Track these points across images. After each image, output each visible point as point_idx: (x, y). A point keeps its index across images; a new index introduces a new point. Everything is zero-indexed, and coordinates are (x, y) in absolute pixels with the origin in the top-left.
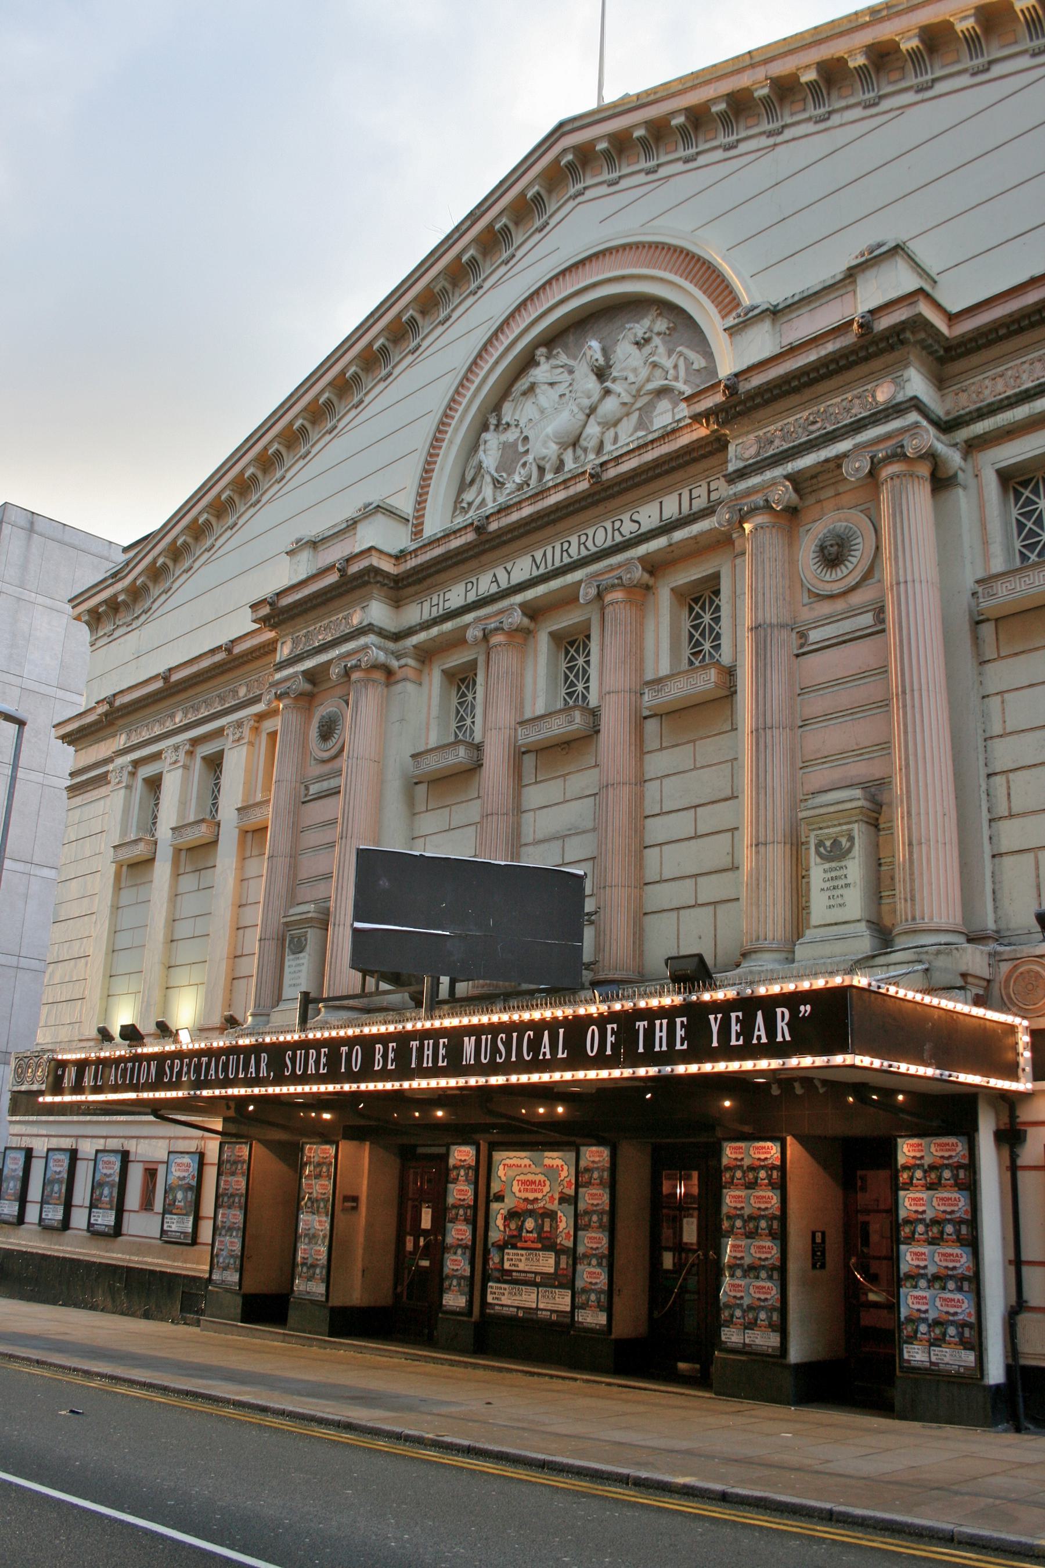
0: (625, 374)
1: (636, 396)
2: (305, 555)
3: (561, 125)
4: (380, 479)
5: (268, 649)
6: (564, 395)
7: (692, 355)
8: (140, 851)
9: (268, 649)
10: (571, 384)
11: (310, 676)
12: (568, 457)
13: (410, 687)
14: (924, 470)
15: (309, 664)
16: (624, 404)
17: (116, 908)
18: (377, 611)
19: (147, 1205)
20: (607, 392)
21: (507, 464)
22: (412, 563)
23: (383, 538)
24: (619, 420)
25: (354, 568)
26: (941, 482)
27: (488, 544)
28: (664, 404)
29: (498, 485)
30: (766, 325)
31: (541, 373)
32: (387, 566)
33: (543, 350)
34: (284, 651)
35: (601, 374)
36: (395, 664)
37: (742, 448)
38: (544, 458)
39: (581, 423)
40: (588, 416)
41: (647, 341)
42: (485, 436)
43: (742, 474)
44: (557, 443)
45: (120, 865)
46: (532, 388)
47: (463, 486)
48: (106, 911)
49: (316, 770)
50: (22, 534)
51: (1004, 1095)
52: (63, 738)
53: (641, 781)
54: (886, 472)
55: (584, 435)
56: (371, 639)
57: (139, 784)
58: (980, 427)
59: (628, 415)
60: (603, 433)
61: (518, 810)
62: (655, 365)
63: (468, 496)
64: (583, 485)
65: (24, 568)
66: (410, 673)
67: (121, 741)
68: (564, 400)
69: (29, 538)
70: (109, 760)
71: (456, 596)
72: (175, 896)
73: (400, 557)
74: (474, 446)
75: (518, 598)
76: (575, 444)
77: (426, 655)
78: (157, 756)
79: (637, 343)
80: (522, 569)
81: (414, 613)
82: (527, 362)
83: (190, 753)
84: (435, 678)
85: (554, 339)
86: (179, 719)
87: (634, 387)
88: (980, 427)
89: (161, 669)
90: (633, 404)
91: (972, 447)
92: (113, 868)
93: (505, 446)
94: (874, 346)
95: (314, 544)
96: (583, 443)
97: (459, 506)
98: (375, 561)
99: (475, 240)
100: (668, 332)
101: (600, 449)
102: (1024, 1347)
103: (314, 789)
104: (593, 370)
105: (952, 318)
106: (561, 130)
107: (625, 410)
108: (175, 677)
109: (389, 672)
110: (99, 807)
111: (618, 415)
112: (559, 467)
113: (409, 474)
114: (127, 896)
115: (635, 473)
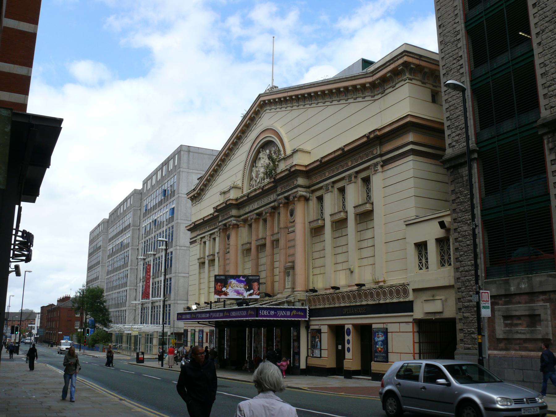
2: (223, 195)
3: (260, 95)
4: (234, 179)
5: (217, 216)
8: (202, 260)
9: (217, 216)
11: (225, 225)
13: (242, 228)
14: (302, 199)
15: (224, 222)
17: (200, 273)
18: (234, 212)
19: (207, 342)
21: (257, 177)
22: (239, 201)
23: (233, 195)
25: (228, 203)
26: (307, 199)
27: (249, 199)
29: (256, 181)
30: (283, 161)
31: (261, 155)
32: (234, 202)
33: (261, 149)
34: (220, 219)
36: (239, 223)
37: (279, 190)
42: (253, 169)
43: (278, 195)
45: (200, 263)
46: (260, 158)
47: (251, 179)
48: (198, 274)
49: (227, 246)
50: (187, 153)
51: (305, 320)
52: (188, 230)
53: (273, 254)
54: (296, 199)
56: (232, 219)
57: (202, 243)
58: (313, 188)
61: (258, 258)
63: (251, 183)
64: (261, 190)
65: (188, 163)
66: (242, 225)
67: (198, 232)
69: (189, 154)
70: (196, 237)
71: (247, 209)
72: (209, 271)
73: (237, 200)
74: (251, 171)
75: (256, 212)
77: (245, 221)
78: (204, 237)
80: (255, 205)
81: (242, 212)
82: (258, 152)
83: (210, 237)
84: (247, 226)
86: (208, 229)
88: (313, 188)
89: (202, 217)
91: (313, 192)
92: (198, 264)
93: (257, 172)
94: (293, 174)
95: (224, 193)
97: (251, 185)
98: (231, 202)
99: (249, 119)
102: (308, 362)
103: (227, 250)
105: (306, 166)
106: (260, 96)
108: (205, 219)
109: (238, 225)
110: (195, 248)
113: (240, 175)
114: (202, 270)
115: (269, 188)
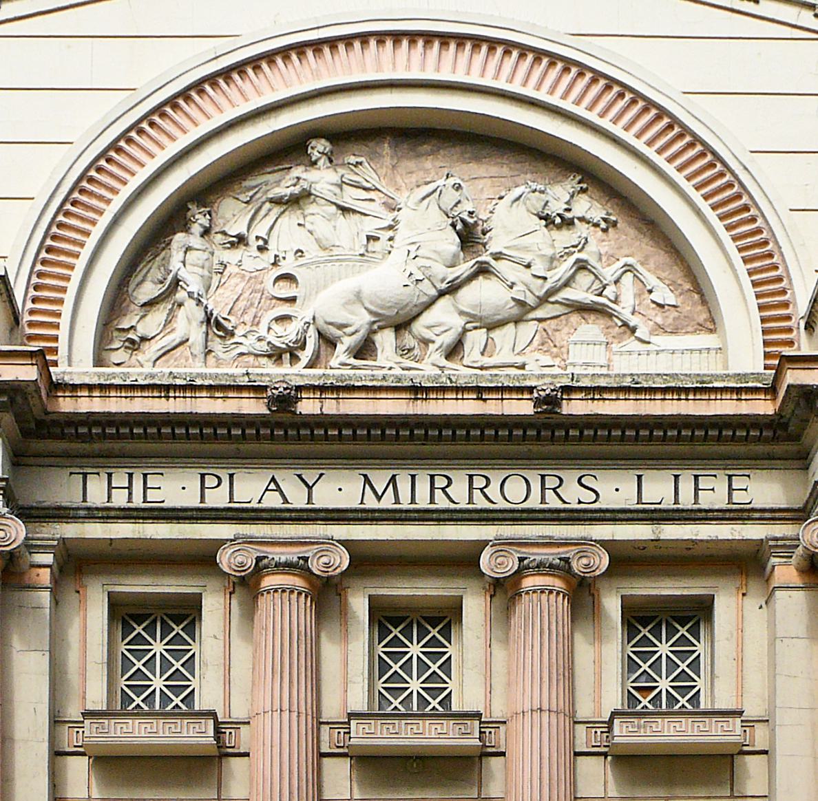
0: (528, 258)
1: (543, 300)
6: (377, 239)
7: (651, 280)
10: (390, 227)
12: (386, 340)
16: (520, 303)
20: (483, 270)
24: (501, 324)
28: (591, 329)
35: (469, 236)
38: (341, 327)
39: (424, 299)
40: (442, 294)
41: (568, 223)
44: (371, 312)
55: (427, 318)
59: (517, 321)
60: (465, 331)
62: (582, 266)
68: (374, 246)
76: (402, 325)
79: (546, 218)
85: (349, 135)
87: (541, 289)
90: (533, 309)
96: (419, 327)
100: (603, 225)
101: (454, 350)
104: (453, 225)
107: (516, 311)
111: (504, 315)
112: (365, 350)
